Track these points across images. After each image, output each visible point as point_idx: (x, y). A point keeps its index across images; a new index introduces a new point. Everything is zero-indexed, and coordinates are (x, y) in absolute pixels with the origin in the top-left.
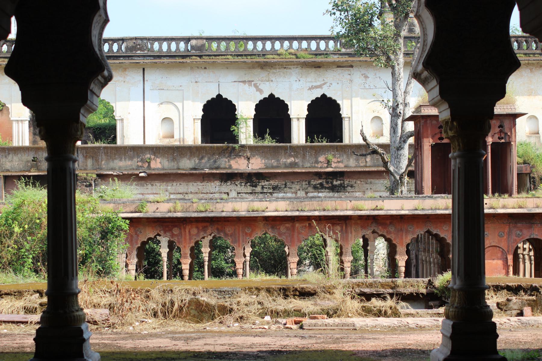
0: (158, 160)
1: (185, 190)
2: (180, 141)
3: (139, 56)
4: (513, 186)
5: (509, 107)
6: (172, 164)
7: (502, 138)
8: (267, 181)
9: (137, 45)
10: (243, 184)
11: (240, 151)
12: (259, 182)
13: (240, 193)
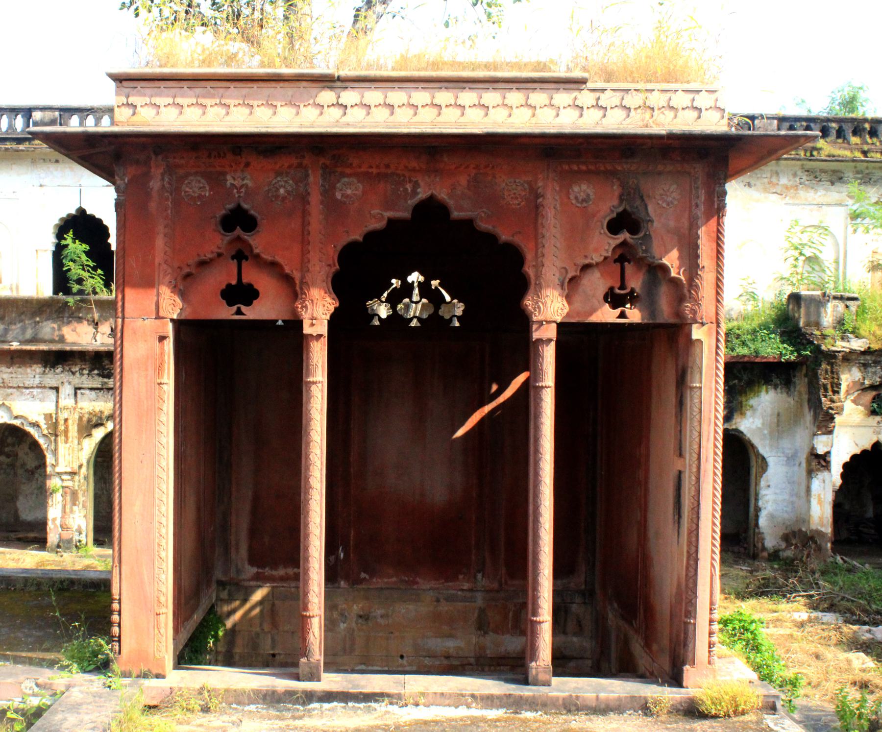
2: (11, 289)
7: (632, 298)
11: (79, 309)
13: (80, 389)
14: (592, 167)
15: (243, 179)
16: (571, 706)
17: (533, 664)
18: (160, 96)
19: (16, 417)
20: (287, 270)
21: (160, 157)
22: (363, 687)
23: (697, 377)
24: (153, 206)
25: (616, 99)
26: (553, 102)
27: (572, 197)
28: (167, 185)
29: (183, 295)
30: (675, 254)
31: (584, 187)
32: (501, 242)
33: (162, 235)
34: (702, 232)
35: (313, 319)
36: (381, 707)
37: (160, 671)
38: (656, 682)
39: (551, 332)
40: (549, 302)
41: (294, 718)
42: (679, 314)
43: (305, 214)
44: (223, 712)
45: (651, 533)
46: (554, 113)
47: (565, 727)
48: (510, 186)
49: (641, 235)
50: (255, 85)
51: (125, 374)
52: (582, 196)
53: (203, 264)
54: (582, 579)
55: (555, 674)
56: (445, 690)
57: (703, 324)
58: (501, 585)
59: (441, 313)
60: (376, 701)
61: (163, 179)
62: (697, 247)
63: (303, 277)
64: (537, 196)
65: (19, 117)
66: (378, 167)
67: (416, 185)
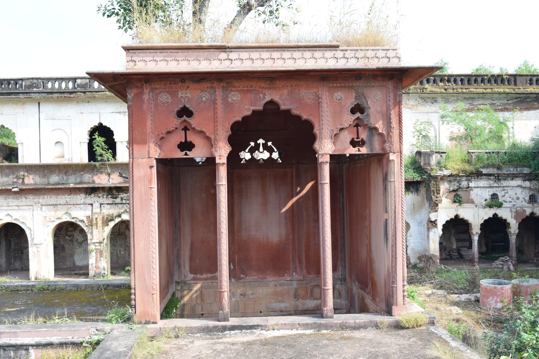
0: (31, 177)
1: (55, 203)
2: (69, 160)
3: (35, 93)
4: (394, 282)
5: (381, 54)
6: (43, 180)
7: (362, 143)
8: (126, 193)
9: (33, 84)
10: (105, 196)
12: (119, 195)
14: (343, 85)
15: (186, 94)
16: (343, 327)
17: (325, 309)
18: (147, 56)
19: (73, 218)
20: (208, 134)
21: (148, 84)
22: (249, 323)
23: (393, 176)
24: (145, 106)
25: (352, 54)
26: (325, 56)
27: (334, 98)
28: (151, 97)
29: (160, 147)
30: (381, 122)
31: (339, 94)
32: (303, 119)
33: (149, 120)
34: (392, 112)
35: (220, 156)
36: (258, 332)
37: (155, 321)
38: (382, 315)
39: (327, 159)
40: (326, 145)
41: (218, 338)
42: (383, 149)
43: (215, 109)
44: (185, 338)
45: (373, 249)
46: (325, 61)
47: (342, 336)
48: (307, 93)
49: (365, 114)
50: (190, 51)
51: (134, 184)
52: (339, 98)
53: (169, 133)
54: (340, 273)
55: (335, 314)
56: (286, 322)
57: (394, 153)
58: (304, 277)
59: (273, 156)
60: (255, 329)
61: (149, 95)
62: (391, 118)
63: (215, 137)
64: (319, 98)
65: (70, 82)
66: (247, 87)
67: (264, 95)
